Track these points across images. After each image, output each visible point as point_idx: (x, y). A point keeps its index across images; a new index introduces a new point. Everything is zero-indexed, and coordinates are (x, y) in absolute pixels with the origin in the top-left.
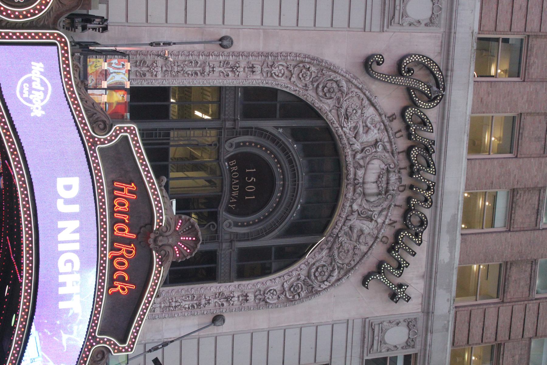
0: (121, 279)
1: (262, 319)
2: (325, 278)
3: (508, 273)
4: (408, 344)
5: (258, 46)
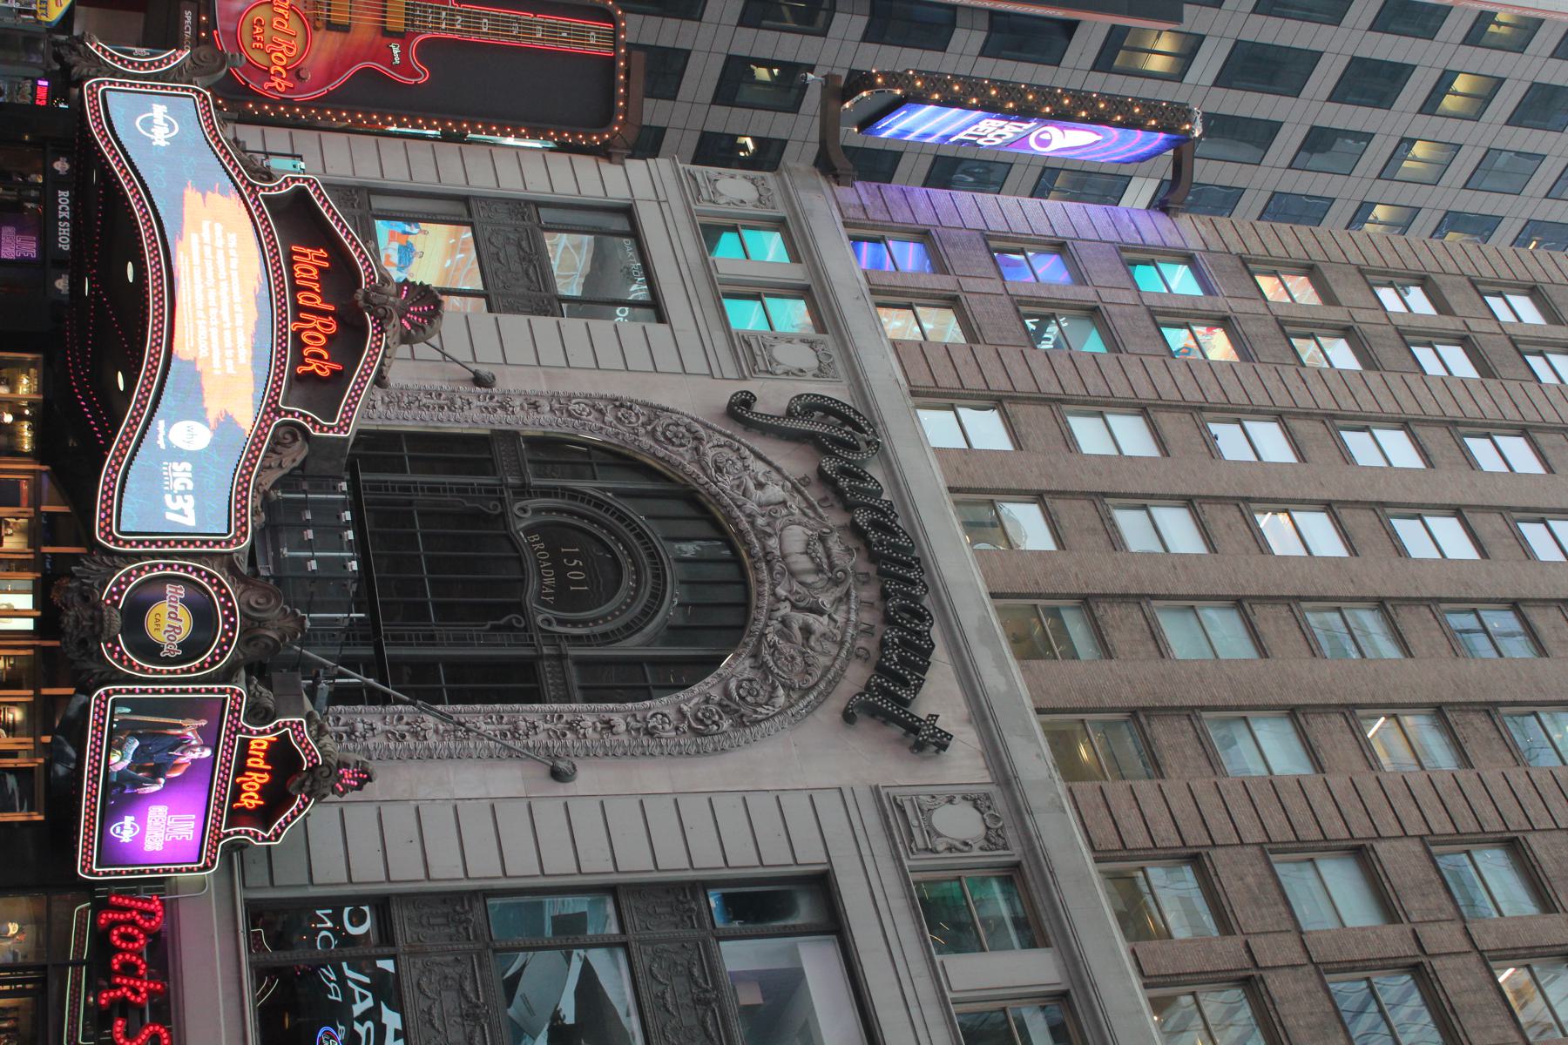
0: (318, 357)
1: (653, 777)
2: (761, 699)
3: (1148, 731)
4: (993, 839)
5: (538, 384)
